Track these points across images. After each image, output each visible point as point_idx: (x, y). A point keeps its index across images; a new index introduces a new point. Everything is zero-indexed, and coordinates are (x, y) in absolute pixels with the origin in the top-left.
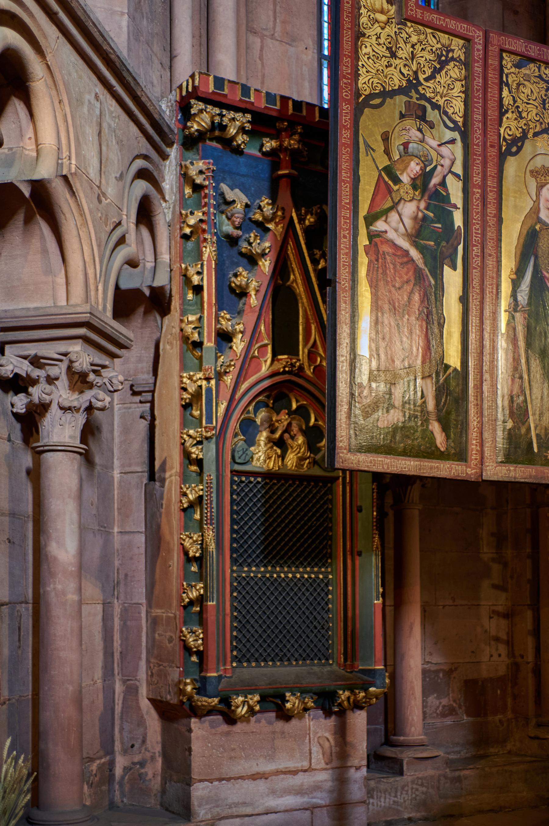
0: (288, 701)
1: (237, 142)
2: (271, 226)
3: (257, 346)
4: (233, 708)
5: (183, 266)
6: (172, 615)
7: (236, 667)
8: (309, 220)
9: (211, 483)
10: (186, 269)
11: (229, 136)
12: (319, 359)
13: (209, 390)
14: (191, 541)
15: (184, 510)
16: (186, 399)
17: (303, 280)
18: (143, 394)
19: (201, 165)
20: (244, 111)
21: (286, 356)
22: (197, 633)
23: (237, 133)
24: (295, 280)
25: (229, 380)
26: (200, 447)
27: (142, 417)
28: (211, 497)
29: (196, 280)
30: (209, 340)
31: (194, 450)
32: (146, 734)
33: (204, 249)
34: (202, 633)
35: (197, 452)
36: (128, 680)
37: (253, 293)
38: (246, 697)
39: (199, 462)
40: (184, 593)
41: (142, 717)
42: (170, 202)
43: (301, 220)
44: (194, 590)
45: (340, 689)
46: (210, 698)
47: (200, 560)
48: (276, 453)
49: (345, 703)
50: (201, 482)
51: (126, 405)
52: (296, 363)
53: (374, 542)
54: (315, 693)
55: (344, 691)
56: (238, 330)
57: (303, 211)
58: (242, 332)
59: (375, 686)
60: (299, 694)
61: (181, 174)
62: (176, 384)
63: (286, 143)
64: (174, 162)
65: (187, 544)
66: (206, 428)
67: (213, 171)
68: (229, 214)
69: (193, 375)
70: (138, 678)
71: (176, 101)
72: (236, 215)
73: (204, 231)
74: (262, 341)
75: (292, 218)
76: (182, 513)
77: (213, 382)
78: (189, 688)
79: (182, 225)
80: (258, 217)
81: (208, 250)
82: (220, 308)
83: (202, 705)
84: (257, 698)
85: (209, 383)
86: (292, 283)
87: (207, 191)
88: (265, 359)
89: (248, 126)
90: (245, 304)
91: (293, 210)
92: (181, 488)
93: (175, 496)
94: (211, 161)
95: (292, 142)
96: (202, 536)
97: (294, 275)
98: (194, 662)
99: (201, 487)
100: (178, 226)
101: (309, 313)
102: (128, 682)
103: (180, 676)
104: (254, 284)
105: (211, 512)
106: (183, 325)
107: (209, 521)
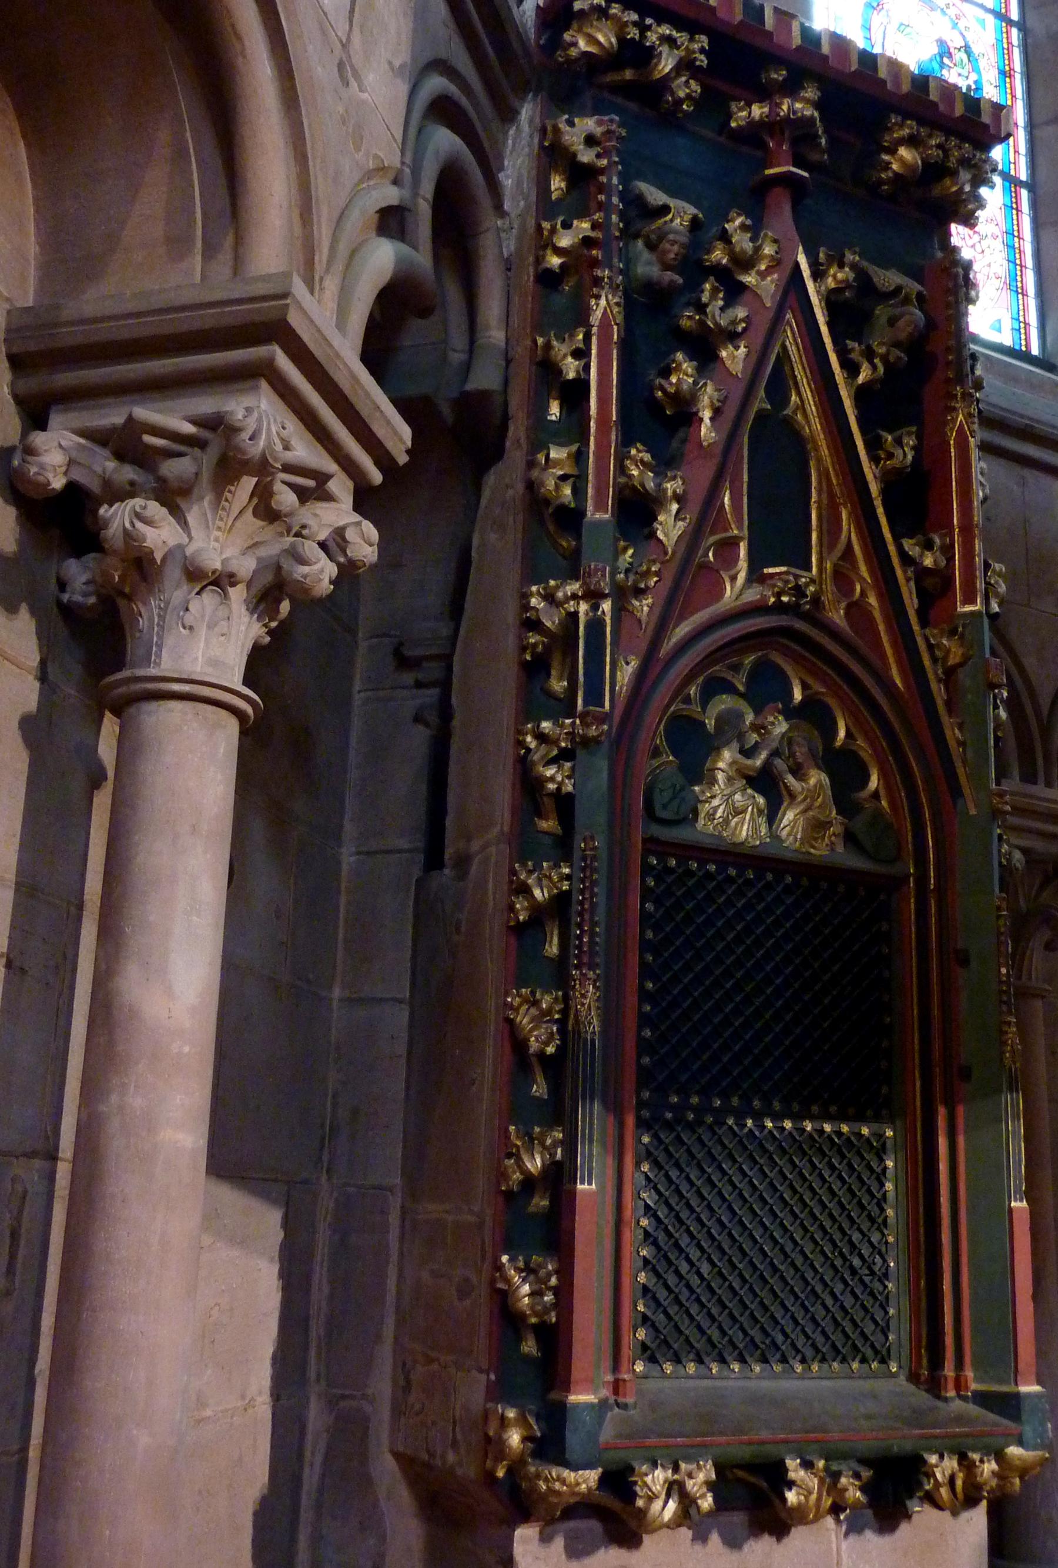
0: (791, 1484)
1: (673, 94)
2: (749, 279)
3: (712, 539)
4: (640, 1503)
5: (540, 341)
6: (472, 1219)
7: (645, 1376)
8: (834, 277)
9: (594, 858)
10: (548, 346)
11: (657, 75)
12: (858, 588)
13: (596, 626)
14: (533, 1011)
15: (519, 930)
16: (535, 645)
17: (820, 405)
18: (425, 664)
19: (589, 124)
20: (692, 28)
21: (783, 569)
22: (542, 1273)
23: (678, 69)
24: (802, 407)
25: (643, 607)
26: (568, 765)
27: (418, 719)
28: (593, 895)
29: (571, 368)
30: (600, 506)
31: (550, 772)
32: (382, 1556)
33: (593, 302)
34: (557, 1272)
35: (559, 778)
36: (343, 1397)
37: (707, 415)
38: (676, 1469)
39: (565, 804)
40: (510, 1155)
41: (375, 1505)
42: (513, 215)
43: (818, 275)
44: (537, 1148)
45: (931, 1451)
46: (575, 1468)
47: (553, 1066)
48: (755, 804)
49: (944, 1492)
50: (567, 858)
51: (381, 693)
52: (807, 585)
53: (1005, 1043)
54: (863, 1461)
55: (942, 1457)
56: (670, 493)
57: (821, 255)
58: (678, 498)
59: (1020, 1443)
60: (821, 1464)
61: (541, 147)
62: (510, 614)
63: (785, 107)
64: (526, 128)
65: (524, 1020)
66: (583, 716)
67: (620, 138)
68: (653, 237)
69: (557, 587)
70: (369, 1391)
71: (538, 6)
72: (671, 237)
73: (595, 263)
74: (726, 530)
75: (797, 265)
76: (513, 940)
77: (606, 606)
78: (514, 1438)
79: (541, 253)
80: (718, 255)
81: (603, 302)
82: (627, 441)
83: (551, 1491)
84: (706, 1472)
85: (595, 607)
86: (795, 412)
87: (604, 179)
88: (732, 572)
89: (702, 60)
90: (684, 441)
91: (801, 248)
92: (513, 872)
93: (494, 892)
94: (617, 118)
95: (798, 106)
96: (566, 999)
97: (799, 394)
98: (527, 1359)
99: (567, 871)
100: (531, 259)
101: (834, 482)
102: (343, 1404)
103: (487, 1400)
104: (708, 395)
105: (593, 934)
106: (535, 473)
107: (585, 960)
